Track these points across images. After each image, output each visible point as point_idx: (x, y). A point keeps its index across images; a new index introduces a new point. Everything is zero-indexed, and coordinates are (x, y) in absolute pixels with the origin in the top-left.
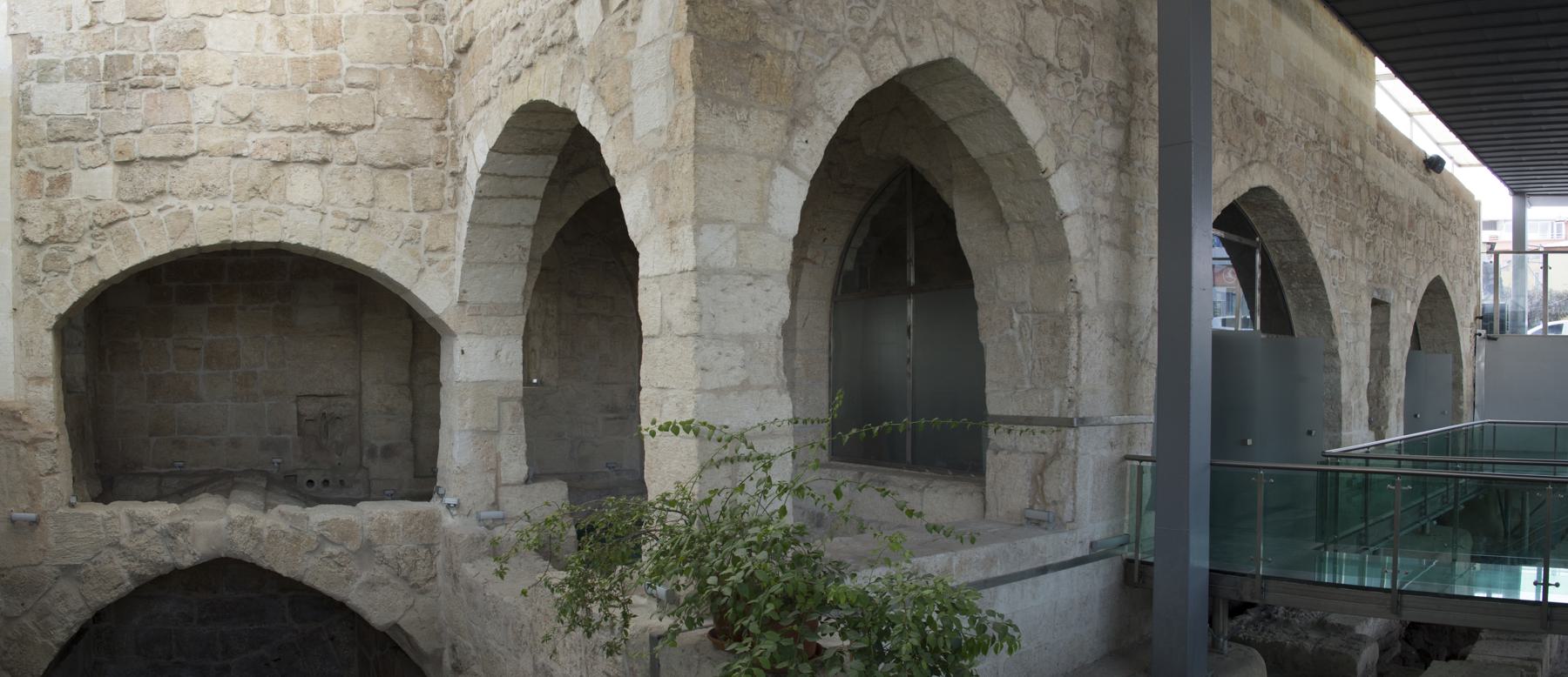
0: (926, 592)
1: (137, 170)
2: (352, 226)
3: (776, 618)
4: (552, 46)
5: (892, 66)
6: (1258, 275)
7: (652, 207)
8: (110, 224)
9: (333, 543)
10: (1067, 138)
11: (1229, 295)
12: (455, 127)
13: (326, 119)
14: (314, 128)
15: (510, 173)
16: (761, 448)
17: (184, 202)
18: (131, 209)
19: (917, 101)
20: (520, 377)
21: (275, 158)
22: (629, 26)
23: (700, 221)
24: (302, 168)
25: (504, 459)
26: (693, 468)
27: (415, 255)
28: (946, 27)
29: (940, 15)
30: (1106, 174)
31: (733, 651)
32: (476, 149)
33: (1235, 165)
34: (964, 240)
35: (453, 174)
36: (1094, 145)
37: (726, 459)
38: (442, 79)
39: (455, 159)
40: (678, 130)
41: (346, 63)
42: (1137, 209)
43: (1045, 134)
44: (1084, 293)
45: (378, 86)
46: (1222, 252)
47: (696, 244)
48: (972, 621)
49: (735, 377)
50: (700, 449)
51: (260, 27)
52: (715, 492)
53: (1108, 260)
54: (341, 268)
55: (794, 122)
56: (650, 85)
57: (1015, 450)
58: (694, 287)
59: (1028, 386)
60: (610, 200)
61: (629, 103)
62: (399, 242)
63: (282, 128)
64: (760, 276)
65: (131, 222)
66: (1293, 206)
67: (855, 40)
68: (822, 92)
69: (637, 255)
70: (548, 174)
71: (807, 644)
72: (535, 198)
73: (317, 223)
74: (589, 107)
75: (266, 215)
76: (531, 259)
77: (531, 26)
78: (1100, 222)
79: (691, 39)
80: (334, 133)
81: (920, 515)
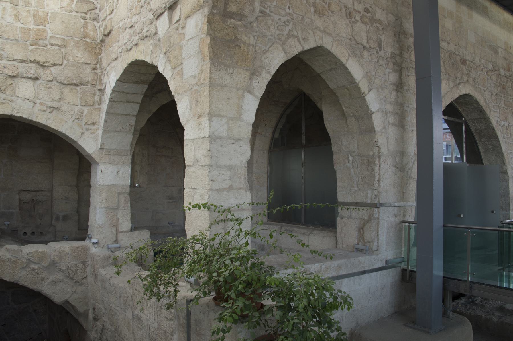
0: (310, 281)
2: (49, 110)
3: (243, 291)
4: (147, 37)
5: (295, 49)
6: (464, 136)
7: (191, 109)
10: (373, 78)
11: (448, 146)
12: (101, 69)
13: (38, 59)
15: (126, 91)
16: (237, 215)
19: (306, 65)
20: (129, 182)
21: (10, 74)
22: (180, 31)
23: (211, 116)
24: (24, 80)
25: (121, 221)
26: (207, 224)
27: (80, 126)
28: (319, 33)
29: (317, 28)
30: (391, 93)
31: (224, 307)
32: (111, 79)
33: (452, 84)
34: (327, 125)
35: (100, 90)
36: (385, 81)
37: (222, 220)
38: (96, 47)
39: (101, 83)
40: (203, 76)
41: (50, 34)
42: (406, 108)
43: (363, 77)
44: (382, 147)
45: (65, 47)
46: (446, 126)
47: (210, 126)
48: (331, 294)
49: (226, 185)
50: (210, 216)
51: (4, 9)
52: (217, 235)
53: (392, 132)
54: (44, 130)
55: (253, 74)
56: (190, 56)
57: (350, 217)
58: (208, 145)
59: (356, 189)
60: (172, 105)
61: (181, 64)
62: (72, 119)
63: (15, 60)
64: (238, 140)
66: (482, 102)
67: (279, 39)
68: (265, 61)
69: (184, 130)
70: (143, 93)
71: (257, 303)
72: (137, 103)
73: (31, 107)
74: (163, 65)
75: (4, 101)
76: (134, 130)
77: (137, 27)
78: (389, 115)
79: (209, 38)
81: (308, 246)
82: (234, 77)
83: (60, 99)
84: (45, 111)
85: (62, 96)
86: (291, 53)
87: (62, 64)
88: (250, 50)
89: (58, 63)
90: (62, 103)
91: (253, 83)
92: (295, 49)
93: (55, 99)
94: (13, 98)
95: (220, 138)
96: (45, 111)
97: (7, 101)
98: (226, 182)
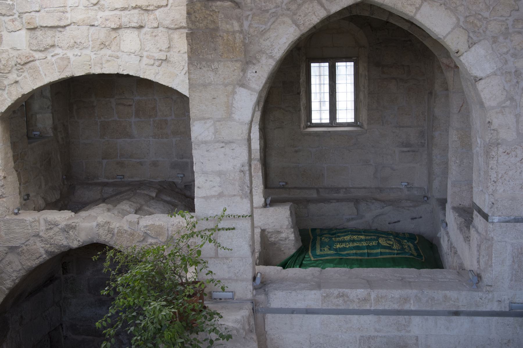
1: (39, 33)
2: (157, 63)
8: (26, 63)
9: (152, 237)
14: (135, 8)
17: (65, 52)
18: (37, 55)
21: (113, 26)
24: (129, 31)
63: (116, 9)
65: (37, 63)
73: (138, 62)
75: (109, 59)
80: (146, 10)
82: (220, 72)
83: (169, 47)
84: (153, 65)
85: (172, 43)
86: (307, 24)
87: (167, 5)
88: (237, 38)
89: (162, 4)
90: (172, 53)
91: (249, 74)
92: (314, 17)
93: (162, 49)
94: (118, 54)
95: (206, 143)
96: (153, 65)
97: (113, 58)
98: (215, 189)
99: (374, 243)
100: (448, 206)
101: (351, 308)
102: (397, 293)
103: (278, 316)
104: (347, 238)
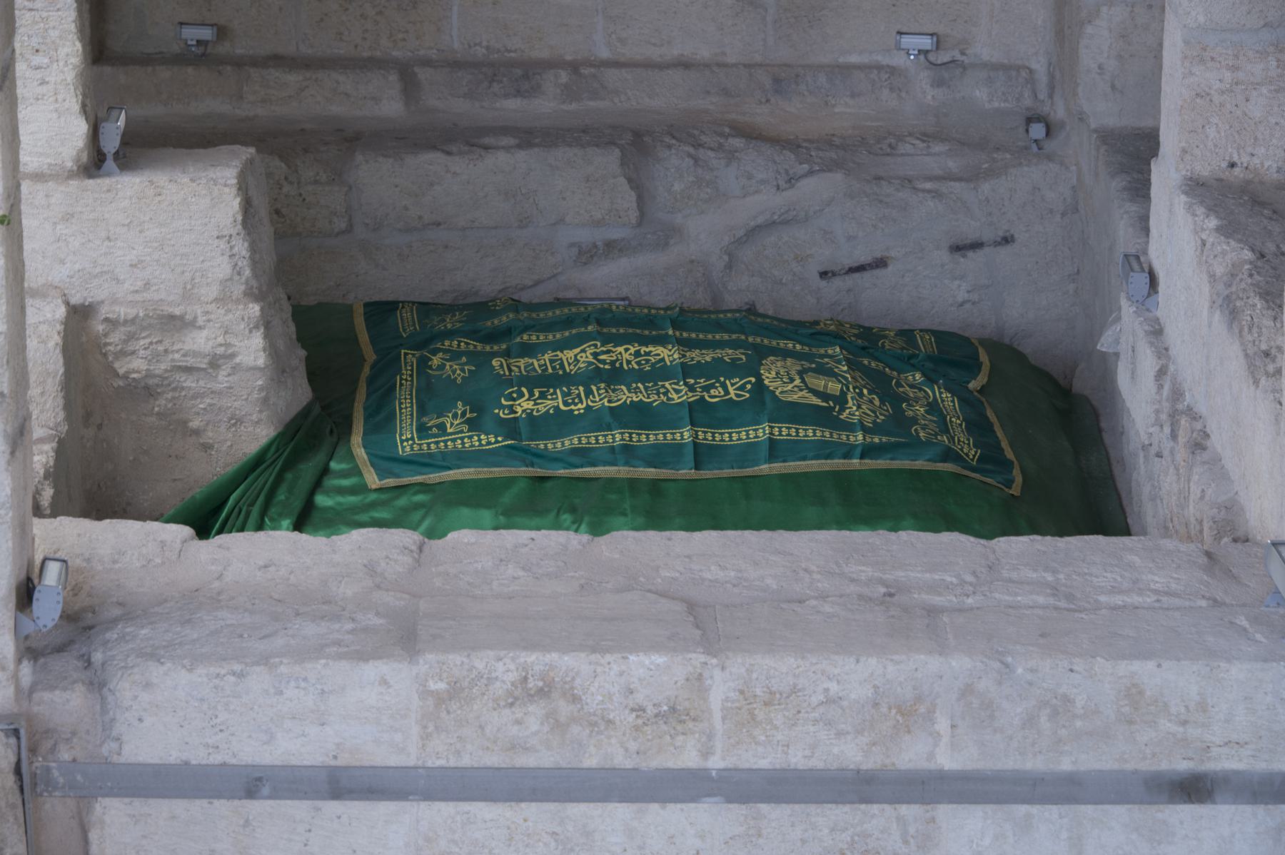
99: (734, 389)
100: (1165, 176)
101: (591, 761)
102: (856, 676)
103: (161, 809)
104: (578, 358)
